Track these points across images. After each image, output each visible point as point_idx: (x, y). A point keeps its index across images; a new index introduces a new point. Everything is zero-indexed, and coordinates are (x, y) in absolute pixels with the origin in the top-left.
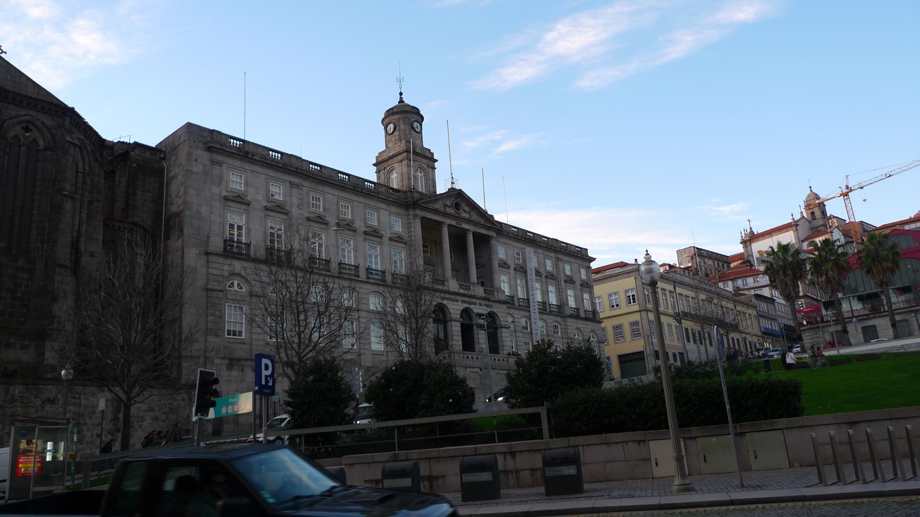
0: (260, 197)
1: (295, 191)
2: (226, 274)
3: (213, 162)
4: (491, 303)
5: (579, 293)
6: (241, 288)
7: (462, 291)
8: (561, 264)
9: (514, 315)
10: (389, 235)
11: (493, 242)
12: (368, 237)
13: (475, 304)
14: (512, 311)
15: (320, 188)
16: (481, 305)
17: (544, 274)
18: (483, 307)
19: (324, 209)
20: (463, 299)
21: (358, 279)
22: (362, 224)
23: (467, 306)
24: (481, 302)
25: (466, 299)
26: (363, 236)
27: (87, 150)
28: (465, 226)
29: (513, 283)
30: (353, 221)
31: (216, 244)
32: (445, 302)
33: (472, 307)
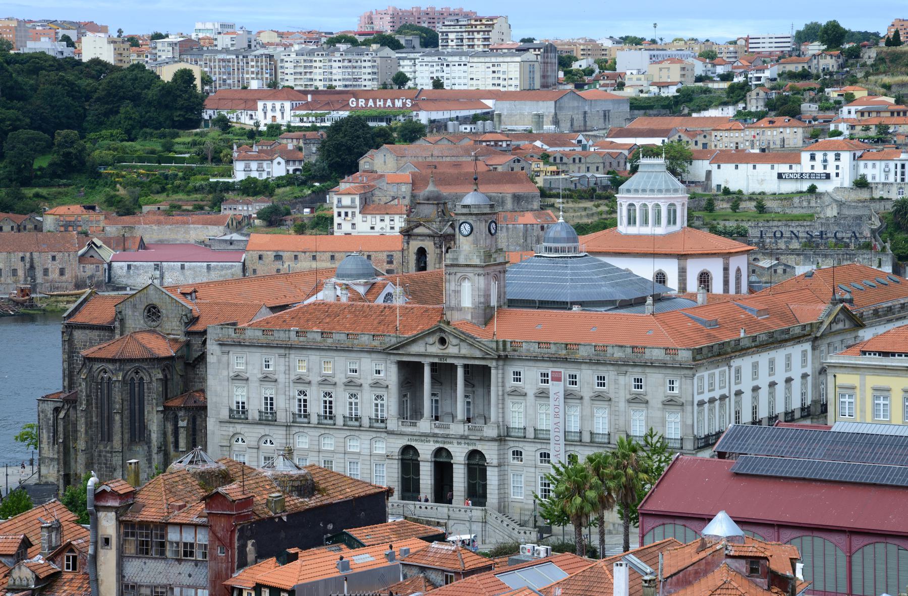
0: (256, 371)
1: (282, 360)
2: (231, 434)
3: (223, 353)
4: (474, 442)
5: (658, 414)
6: (244, 442)
7: (437, 431)
8: (622, 380)
9: (526, 448)
10: (370, 382)
11: (493, 372)
12: (348, 388)
13: (451, 443)
14: (521, 445)
15: (304, 352)
16: (459, 443)
17: (587, 394)
18: (463, 445)
19: (308, 370)
20: (436, 439)
21: (334, 427)
22: (343, 376)
23: (441, 445)
24: (459, 441)
25: (440, 439)
26: (343, 387)
27: (145, 369)
28: (449, 361)
29: (530, 411)
30: (333, 376)
31: (225, 414)
32: (413, 444)
33: (446, 446)
